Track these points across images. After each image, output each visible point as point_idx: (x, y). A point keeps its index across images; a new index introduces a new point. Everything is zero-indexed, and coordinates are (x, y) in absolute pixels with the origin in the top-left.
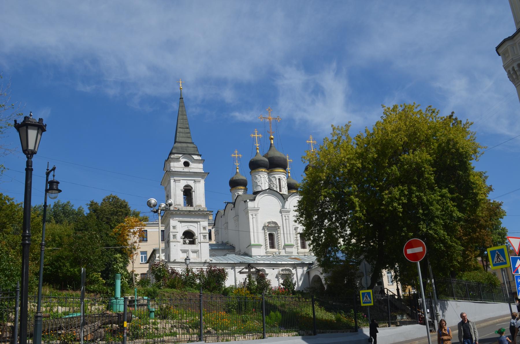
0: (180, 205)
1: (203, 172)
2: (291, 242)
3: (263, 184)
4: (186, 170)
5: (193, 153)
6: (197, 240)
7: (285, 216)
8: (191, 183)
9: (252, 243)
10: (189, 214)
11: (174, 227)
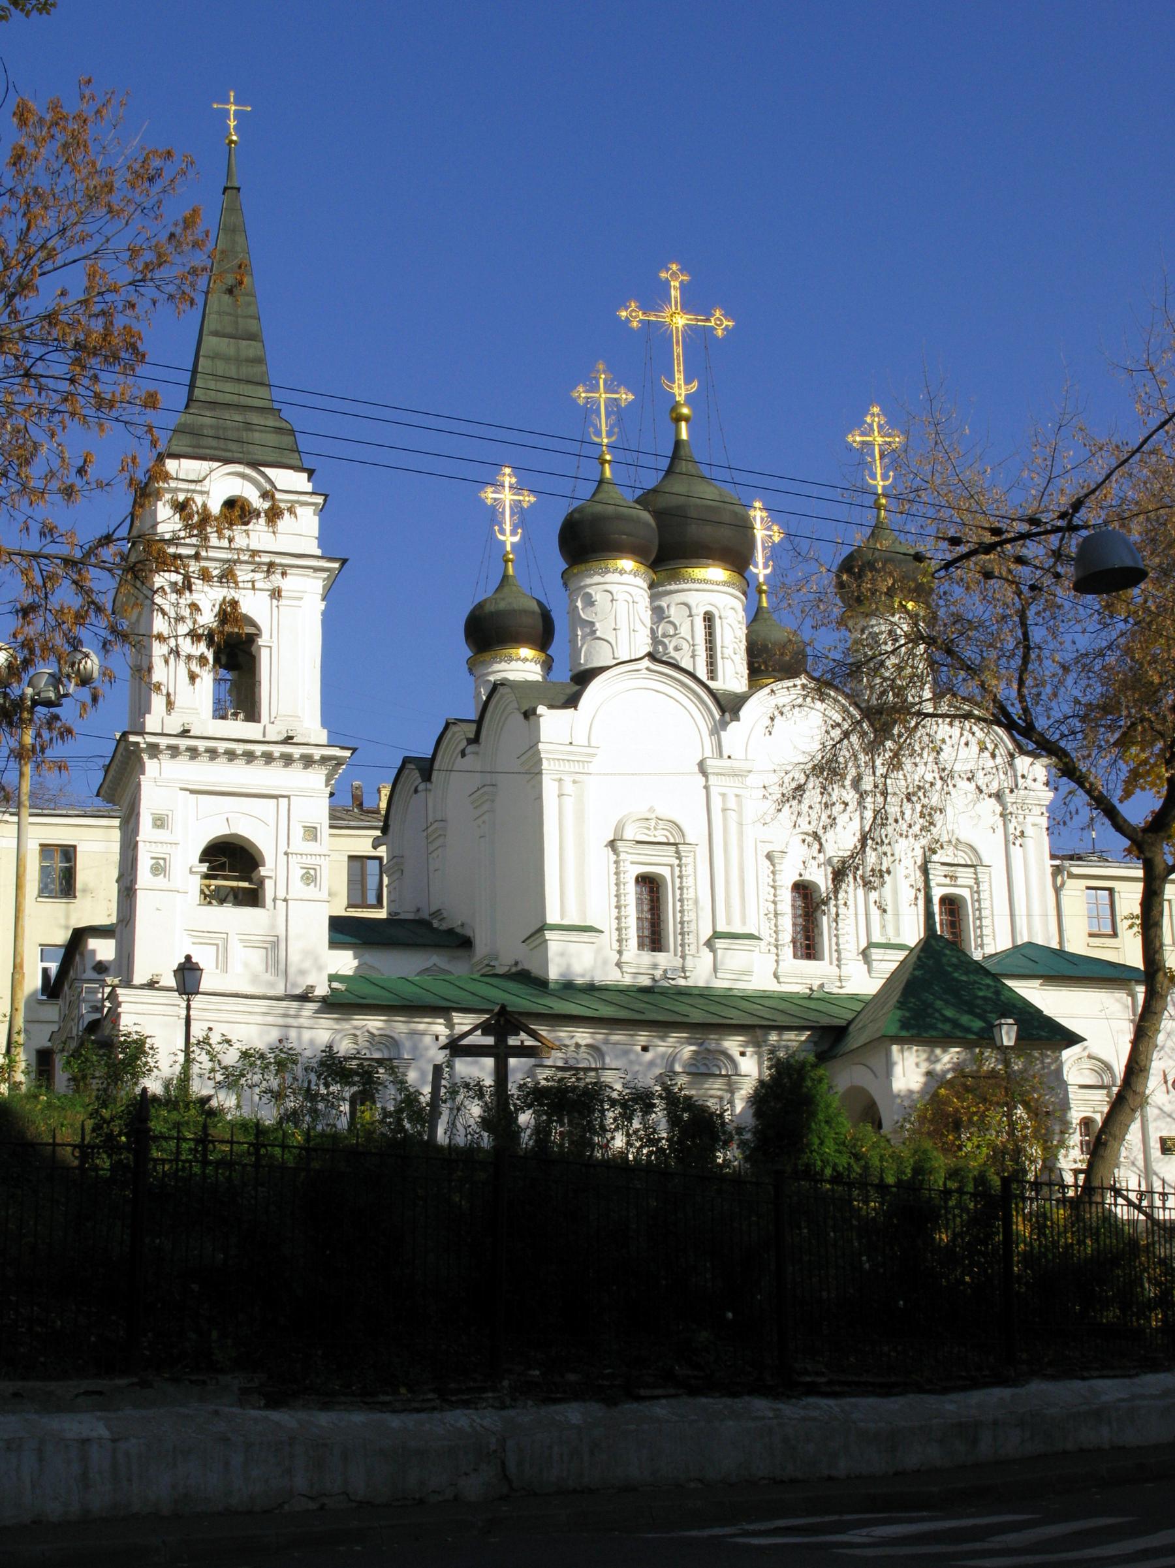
1: (319, 552)
2: (744, 923)
3: (623, 634)
5: (270, 459)
6: (268, 884)
7: (724, 795)
9: (552, 917)
11: (160, 822)
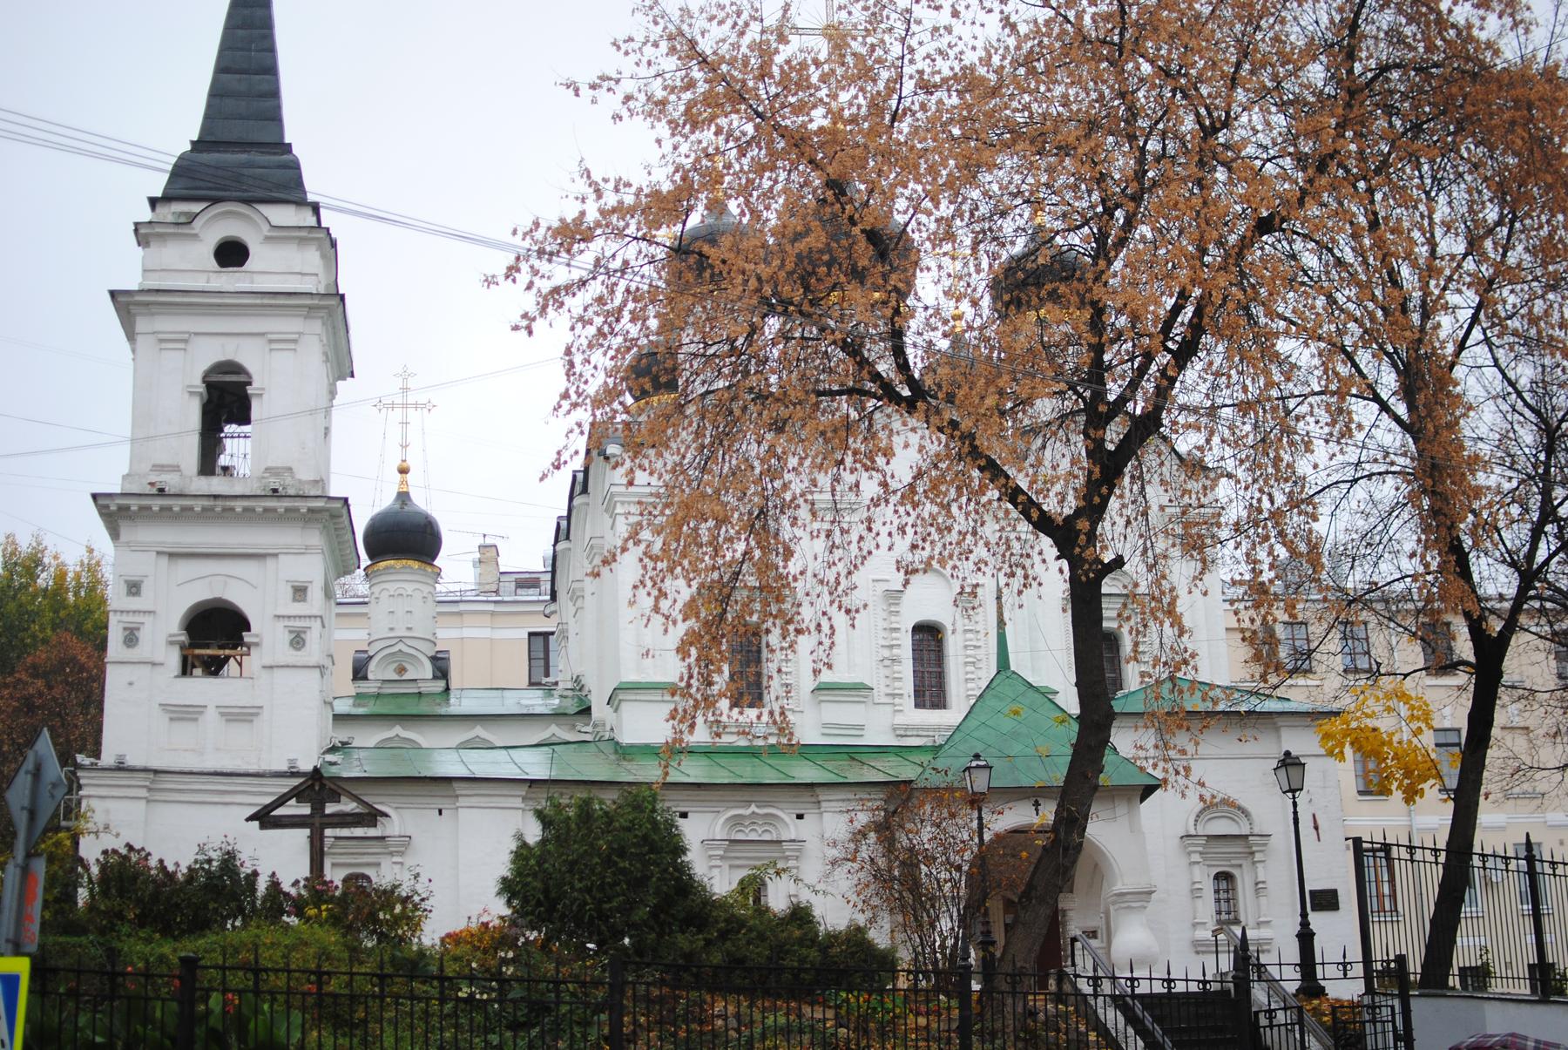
0: (176, 468)
4: (230, 280)
8: (249, 356)
10: (220, 510)
